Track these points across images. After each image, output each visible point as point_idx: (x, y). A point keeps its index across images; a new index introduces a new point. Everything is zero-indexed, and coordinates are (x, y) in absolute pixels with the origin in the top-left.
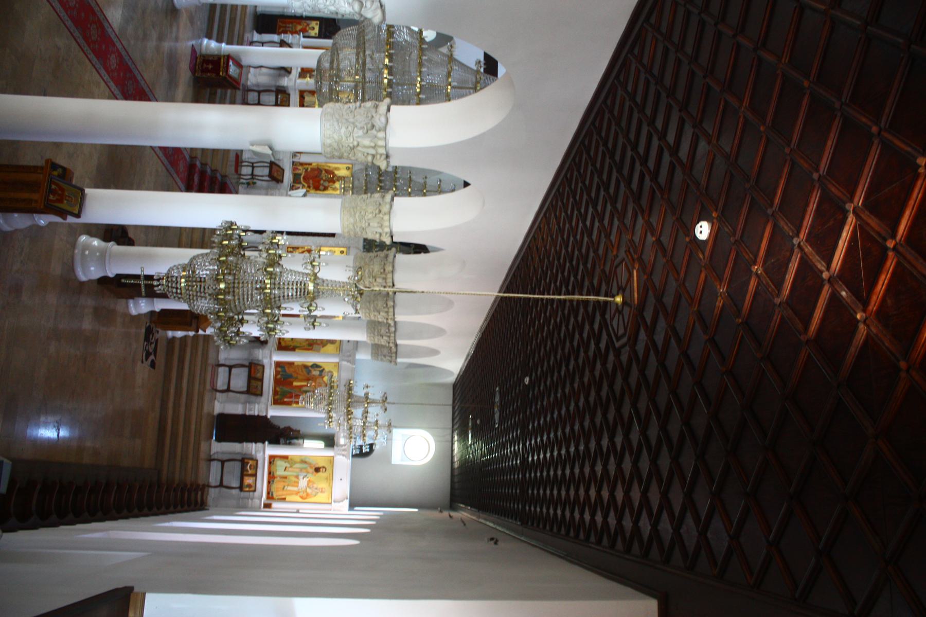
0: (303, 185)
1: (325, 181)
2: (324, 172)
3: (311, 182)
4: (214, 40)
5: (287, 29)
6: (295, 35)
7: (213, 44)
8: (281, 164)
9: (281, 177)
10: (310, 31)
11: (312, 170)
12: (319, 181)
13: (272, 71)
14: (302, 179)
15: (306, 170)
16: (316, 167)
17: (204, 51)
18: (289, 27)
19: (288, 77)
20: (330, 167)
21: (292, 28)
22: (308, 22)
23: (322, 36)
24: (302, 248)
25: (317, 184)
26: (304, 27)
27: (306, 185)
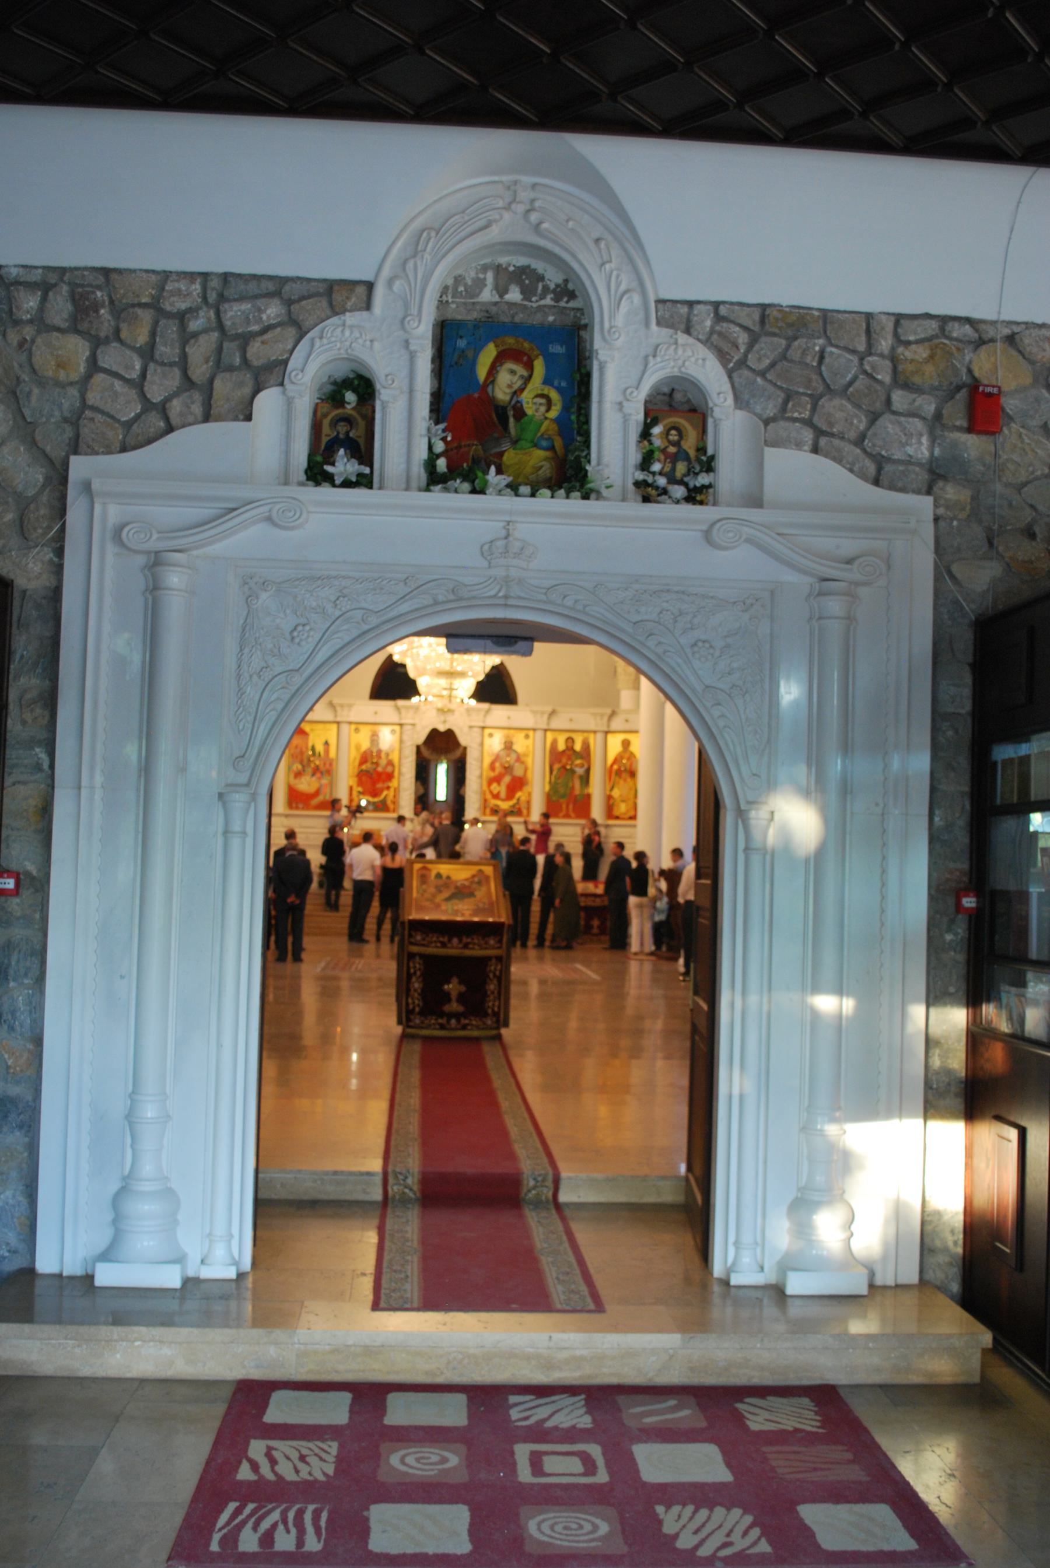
2: (364, 767)
3: (379, 785)
11: (360, 783)
12: (379, 774)
14: (376, 800)
16: (356, 779)
20: (355, 758)
24: (484, 794)
27: (385, 793)
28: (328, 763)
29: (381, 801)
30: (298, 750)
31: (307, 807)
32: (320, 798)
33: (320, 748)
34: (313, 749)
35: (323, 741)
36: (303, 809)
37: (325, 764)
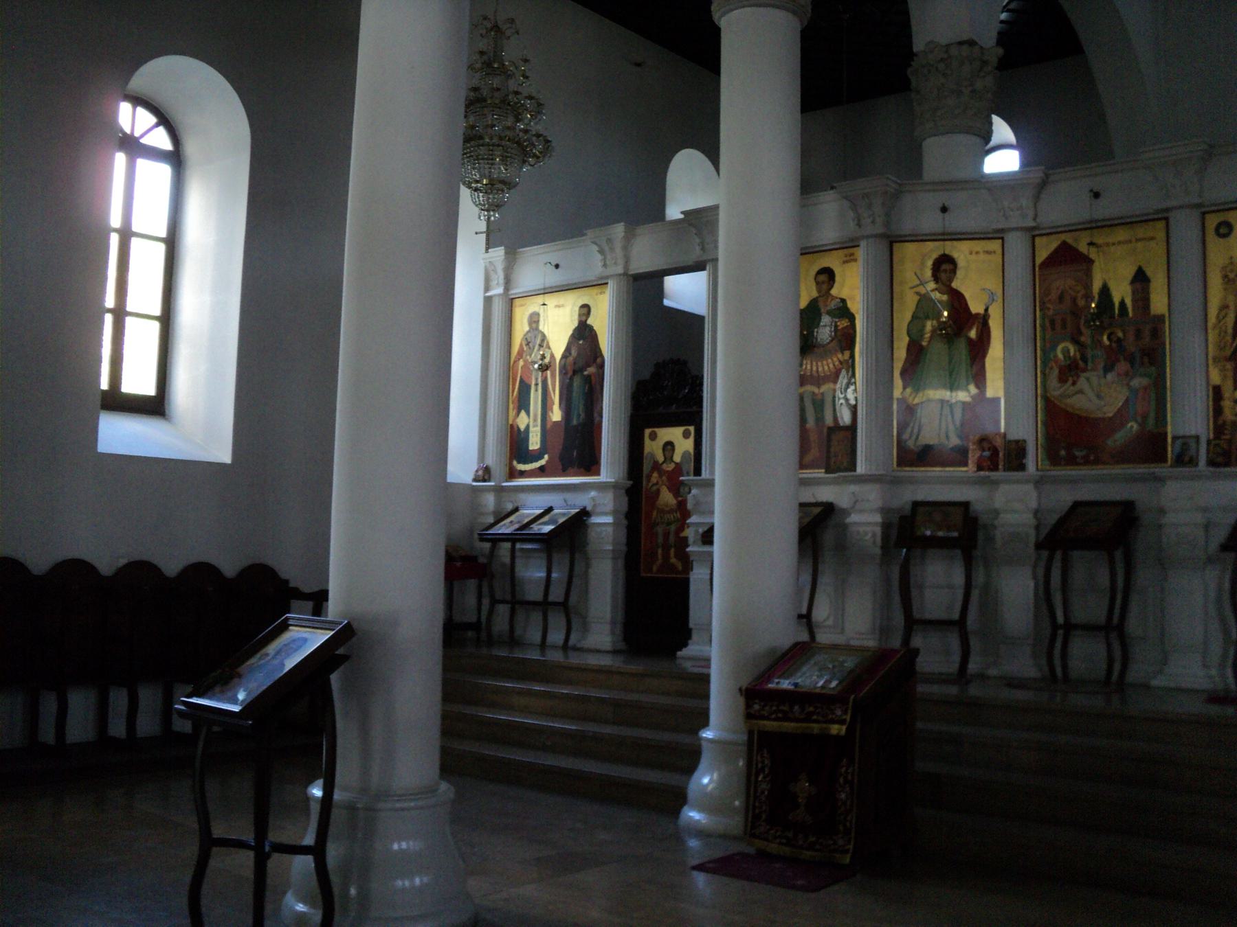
4: (688, 783)
5: (672, 538)
6: (690, 506)
7: (705, 779)
10: (677, 458)
13: (825, 580)
16: (1229, 366)
17: (735, 824)
18: (667, 535)
19: (845, 513)
21: (669, 524)
22: (646, 468)
23: (695, 408)
26: (664, 478)
31: (1094, 456)
33: (1121, 292)
34: (1105, 291)
35: (1128, 271)
36: (1086, 462)
37: (1138, 334)
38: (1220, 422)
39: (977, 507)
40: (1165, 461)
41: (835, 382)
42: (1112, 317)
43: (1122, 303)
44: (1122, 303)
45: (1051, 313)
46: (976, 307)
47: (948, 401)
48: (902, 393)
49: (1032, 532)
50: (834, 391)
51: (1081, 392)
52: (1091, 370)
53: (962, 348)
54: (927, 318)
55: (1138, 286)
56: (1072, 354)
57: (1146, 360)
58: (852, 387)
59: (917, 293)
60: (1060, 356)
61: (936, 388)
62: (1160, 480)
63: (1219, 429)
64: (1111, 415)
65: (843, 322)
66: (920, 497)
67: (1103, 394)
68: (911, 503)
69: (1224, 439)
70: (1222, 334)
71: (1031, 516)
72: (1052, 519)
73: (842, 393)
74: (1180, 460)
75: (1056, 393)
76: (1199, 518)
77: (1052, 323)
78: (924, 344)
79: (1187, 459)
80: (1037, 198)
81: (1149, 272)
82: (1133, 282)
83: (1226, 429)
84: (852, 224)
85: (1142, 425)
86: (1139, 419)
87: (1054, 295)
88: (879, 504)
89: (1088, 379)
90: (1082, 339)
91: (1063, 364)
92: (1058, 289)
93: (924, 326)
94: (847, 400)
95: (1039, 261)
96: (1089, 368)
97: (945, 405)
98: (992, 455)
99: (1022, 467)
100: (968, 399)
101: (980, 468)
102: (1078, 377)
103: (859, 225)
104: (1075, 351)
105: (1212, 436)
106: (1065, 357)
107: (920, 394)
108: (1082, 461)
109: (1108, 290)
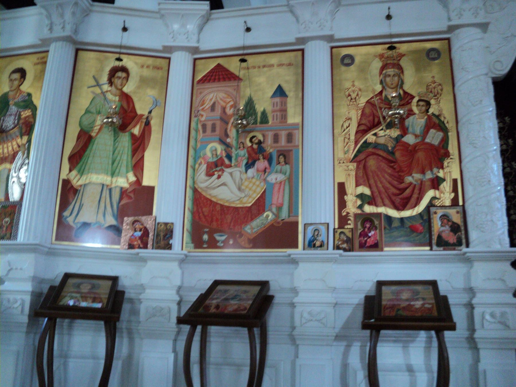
0: (431, 204)
1: (405, 131)
8: (359, 299)
9: (419, 288)
14: (407, 213)
15: (372, 201)
16: (353, 166)
25: (420, 155)
27: (430, 194)
28: (283, 135)
29: (420, 215)
30: (218, 112)
32: (269, 216)
34: (250, 104)
37: (276, 138)
38: (344, 214)
39: (125, 283)
40: (296, 246)
41: (12, 162)
42: (255, 123)
43: (264, 113)
44: (264, 113)
45: (203, 119)
46: (141, 109)
47: (107, 186)
48: (68, 174)
49: (175, 307)
50: (10, 170)
51: (224, 184)
52: (236, 166)
53: (125, 140)
54: (99, 113)
55: (277, 100)
56: (219, 153)
57: (282, 159)
58: (25, 168)
59: (93, 92)
60: (209, 154)
61: (97, 173)
62: (294, 262)
63: (343, 220)
64: (250, 205)
65: (26, 112)
66: (73, 270)
67: (243, 187)
68: (63, 274)
69: (347, 228)
70: (346, 140)
71: (174, 292)
72: (193, 297)
73: (15, 172)
74: (311, 244)
75: (203, 185)
76: (329, 298)
77: (204, 127)
78: (93, 134)
79: (318, 244)
80: (201, 29)
81: (286, 87)
82: (274, 95)
83: (350, 220)
84: (46, 31)
85: (277, 216)
86: (274, 210)
87: (208, 105)
88: (32, 274)
89: (231, 174)
90: (228, 140)
91: (211, 160)
92: (211, 100)
93: (94, 121)
94: (19, 178)
95: (199, 77)
96: (233, 165)
97: (105, 188)
98: (142, 235)
99: (169, 247)
100: (126, 185)
101: (131, 246)
102: (223, 171)
103: (51, 29)
104: (222, 150)
105: (337, 227)
106: (213, 155)
107: (84, 177)
108: (222, 245)
109: (253, 102)
